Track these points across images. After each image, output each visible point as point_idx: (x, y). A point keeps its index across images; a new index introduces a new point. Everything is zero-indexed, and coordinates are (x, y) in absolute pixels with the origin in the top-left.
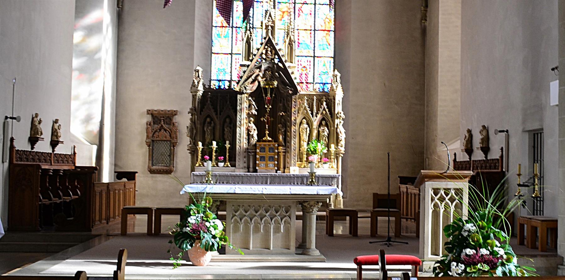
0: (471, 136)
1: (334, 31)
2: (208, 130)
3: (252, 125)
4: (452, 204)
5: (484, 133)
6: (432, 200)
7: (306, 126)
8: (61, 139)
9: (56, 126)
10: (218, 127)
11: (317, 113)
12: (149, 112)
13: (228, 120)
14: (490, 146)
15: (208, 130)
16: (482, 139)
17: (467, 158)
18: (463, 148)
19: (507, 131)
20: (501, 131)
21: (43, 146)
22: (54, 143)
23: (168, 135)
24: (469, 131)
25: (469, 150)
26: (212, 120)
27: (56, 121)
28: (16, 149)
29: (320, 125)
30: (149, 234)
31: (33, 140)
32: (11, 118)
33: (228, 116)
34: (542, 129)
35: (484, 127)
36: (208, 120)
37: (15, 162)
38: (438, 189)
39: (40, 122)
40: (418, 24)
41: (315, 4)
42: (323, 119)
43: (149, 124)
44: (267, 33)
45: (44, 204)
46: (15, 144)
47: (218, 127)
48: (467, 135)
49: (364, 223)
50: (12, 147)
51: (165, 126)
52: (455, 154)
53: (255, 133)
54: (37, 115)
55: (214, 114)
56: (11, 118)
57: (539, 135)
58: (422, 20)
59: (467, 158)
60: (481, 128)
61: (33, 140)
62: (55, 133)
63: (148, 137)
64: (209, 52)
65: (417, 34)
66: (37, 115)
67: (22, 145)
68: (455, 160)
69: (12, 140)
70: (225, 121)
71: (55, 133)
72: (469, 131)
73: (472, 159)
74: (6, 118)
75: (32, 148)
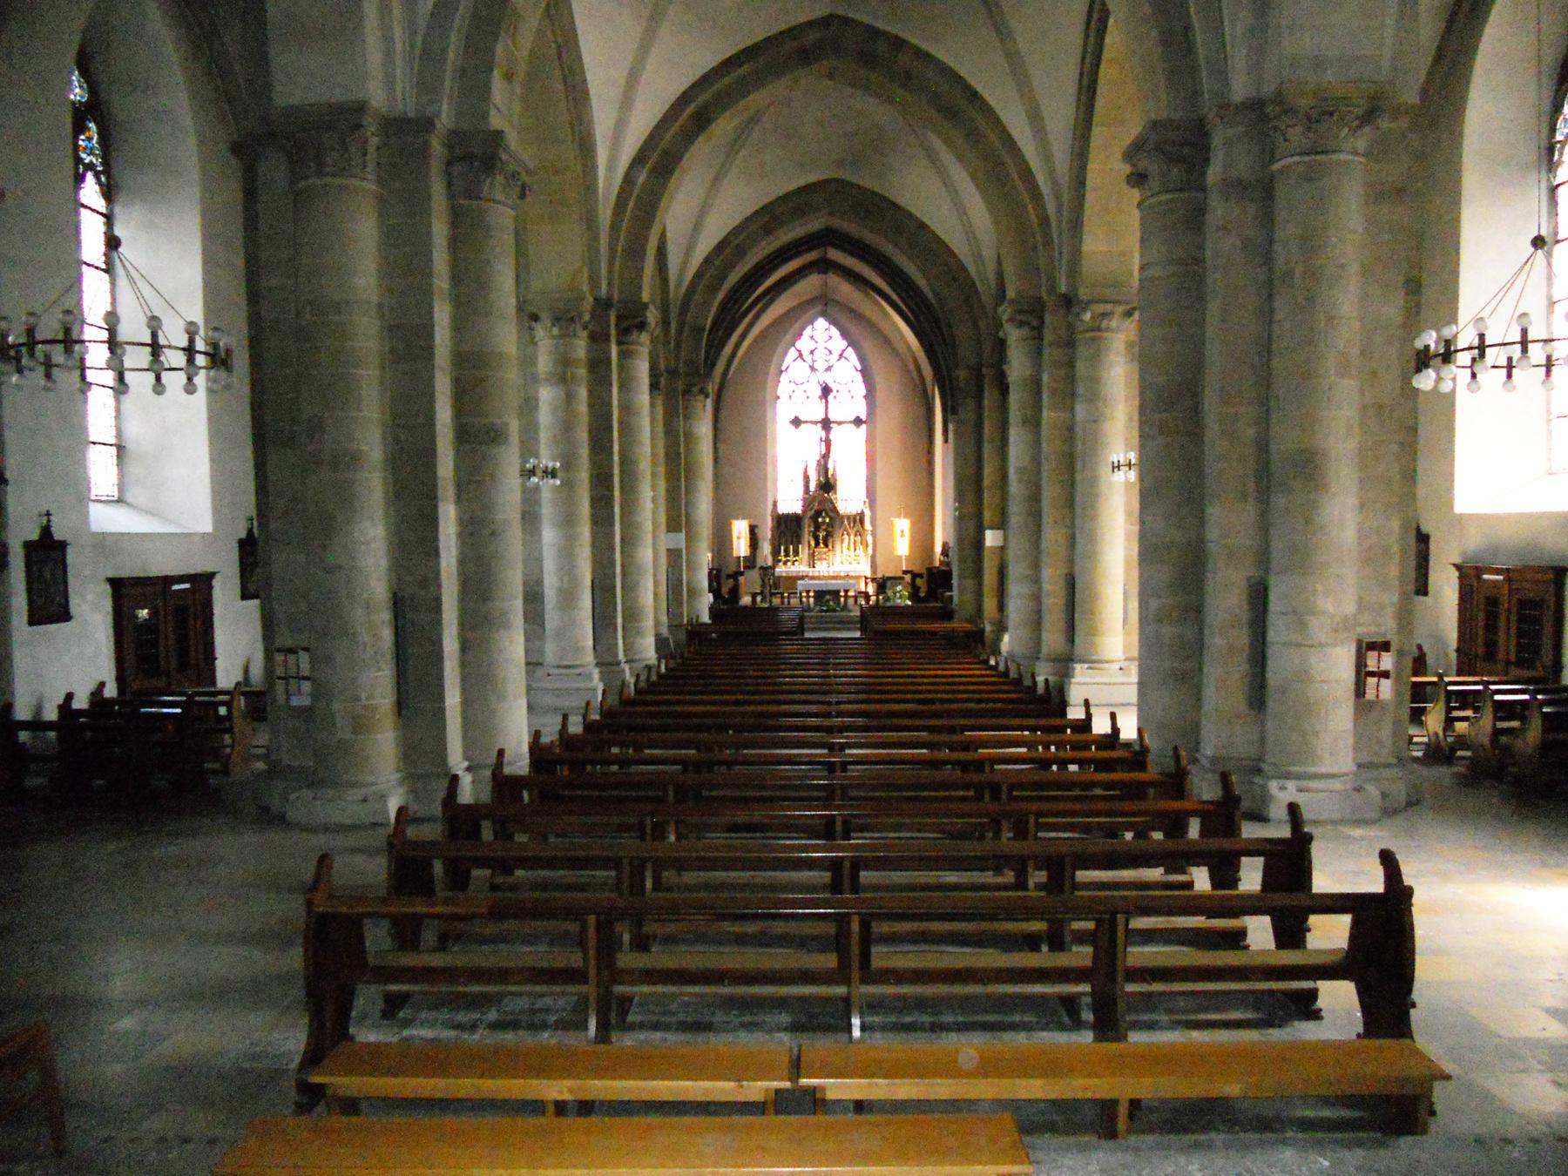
7: (846, 537)
53: (813, 543)
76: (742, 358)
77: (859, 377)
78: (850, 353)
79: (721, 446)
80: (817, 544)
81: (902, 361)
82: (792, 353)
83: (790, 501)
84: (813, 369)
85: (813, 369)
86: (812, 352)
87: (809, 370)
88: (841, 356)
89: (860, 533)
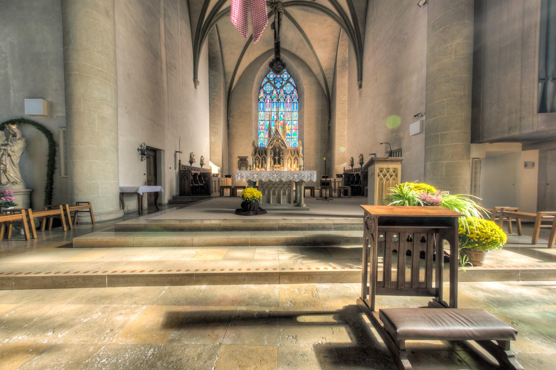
0: (353, 160)
1: (298, 129)
2: (257, 162)
3: (272, 160)
4: (384, 178)
5: (361, 157)
6: (379, 175)
7: (289, 160)
8: (204, 163)
9: (202, 158)
10: (261, 161)
11: (294, 155)
12: (239, 157)
13: (264, 158)
14: (364, 162)
15: (257, 162)
16: (360, 159)
17: (350, 168)
18: (350, 164)
19: (375, 154)
20: (372, 154)
21: (197, 164)
22: (202, 165)
23: (245, 164)
24: (352, 158)
25: (352, 165)
26: (258, 158)
27: (202, 157)
28: (183, 164)
29: (295, 159)
30: (231, 196)
31: (191, 162)
32: (178, 152)
33: (264, 157)
34: (401, 149)
35: (361, 155)
36: (257, 158)
37: (181, 169)
38: (382, 168)
39: (194, 156)
40: (327, 125)
41: (292, 120)
42: (296, 157)
43: (239, 161)
44: (276, 128)
45: (195, 186)
46: (181, 162)
47: (261, 161)
48: (351, 160)
49: (317, 192)
50: (180, 164)
51: (244, 162)
52: (344, 168)
53: (273, 163)
54: (192, 153)
55: (259, 156)
56: (178, 152)
57: (400, 152)
58: (328, 123)
59: (350, 168)
60: (359, 155)
61: (191, 162)
62: (202, 161)
63: (238, 165)
64: (257, 137)
65: (327, 129)
66: (192, 153)
67: (185, 162)
68: (344, 170)
69: (180, 161)
70: (263, 159)
71: (202, 161)
72: (352, 158)
73: (353, 168)
74: (176, 152)
75: (191, 165)
76: (240, 78)
77: (295, 93)
78: (291, 80)
79: (231, 119)
80: (275, 163)
81: (317, 79)
82: (266, 80)
83: (263, 140)
84: (276, 88)
85: (276, 88)
86: (274, 79)
87: (272, 88)
88: (288, 81)
89: (296, 159)
